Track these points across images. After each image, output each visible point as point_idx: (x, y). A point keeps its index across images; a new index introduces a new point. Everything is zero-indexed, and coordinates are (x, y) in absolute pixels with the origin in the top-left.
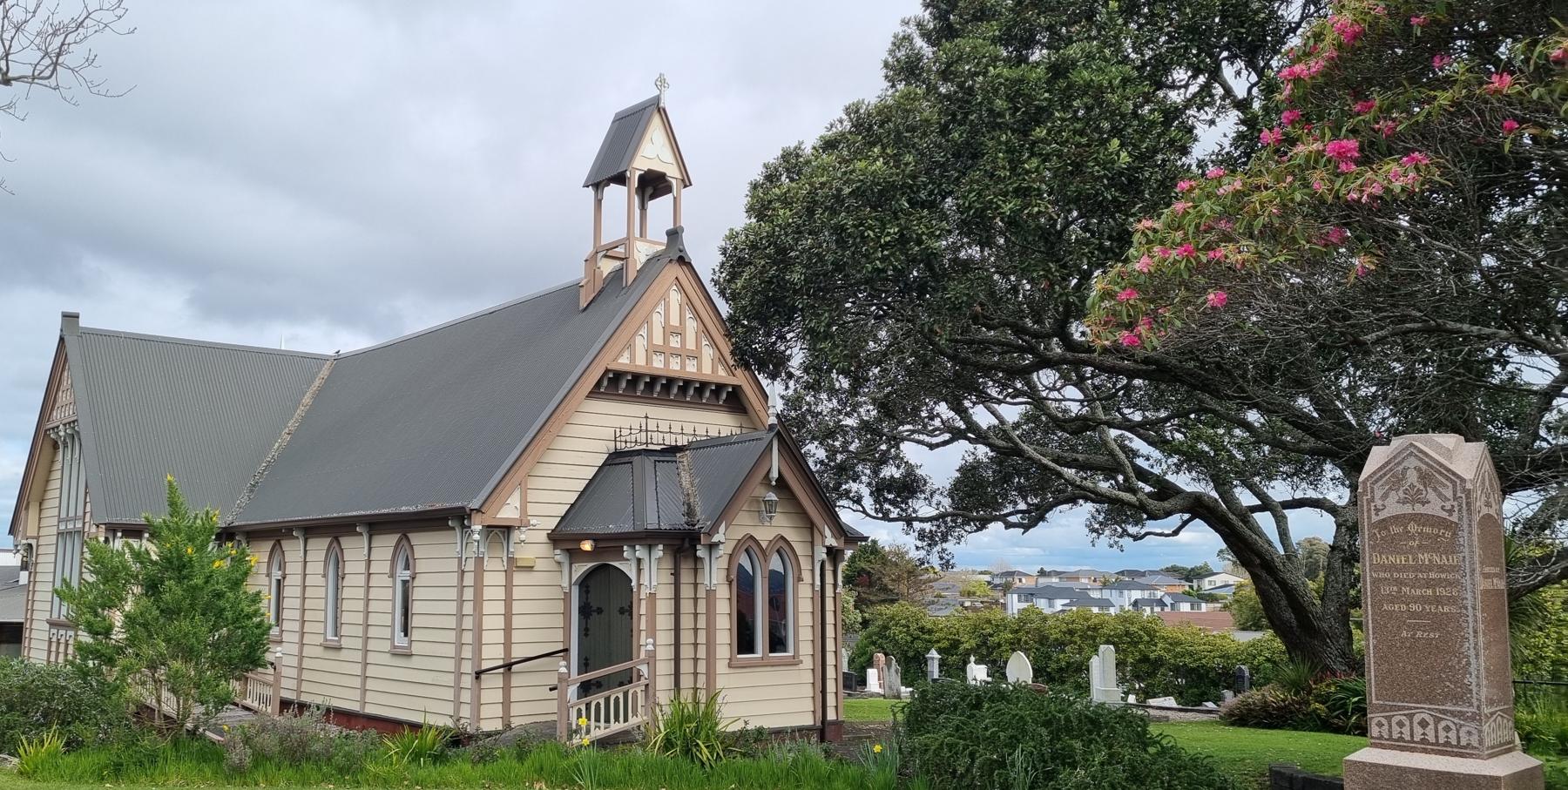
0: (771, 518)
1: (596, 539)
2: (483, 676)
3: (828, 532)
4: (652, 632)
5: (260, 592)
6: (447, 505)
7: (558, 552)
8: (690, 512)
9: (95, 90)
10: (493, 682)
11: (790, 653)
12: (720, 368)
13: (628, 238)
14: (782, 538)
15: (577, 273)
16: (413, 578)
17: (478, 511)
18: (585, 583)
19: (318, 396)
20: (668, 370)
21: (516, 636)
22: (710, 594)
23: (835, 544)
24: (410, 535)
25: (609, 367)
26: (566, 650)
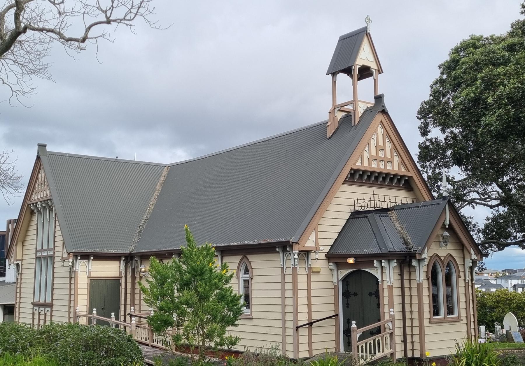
0: (446, 245)
1: (355, 256)
2: (299, 329)
3: (472, 252)
4: (391, 305)
5: (231, 287)
6: (275, 240)
7: (331, 264)
8: (406, 243)
9: (153, 26)
10: (304, 332)
11: (456, 315)
12: (402, 167)
13: (354, 100)
14: (451, 255)
15: (325, 117)
16: (252, 279)
17: (297, 243)
18: (345, 280)
19: (164, 185)
20: (379, 168)
21: (314, 308)
22: (419, 285)
23: (476, 258)
24: (248, 256)
25: (353, 167)
26: (337, 315)
